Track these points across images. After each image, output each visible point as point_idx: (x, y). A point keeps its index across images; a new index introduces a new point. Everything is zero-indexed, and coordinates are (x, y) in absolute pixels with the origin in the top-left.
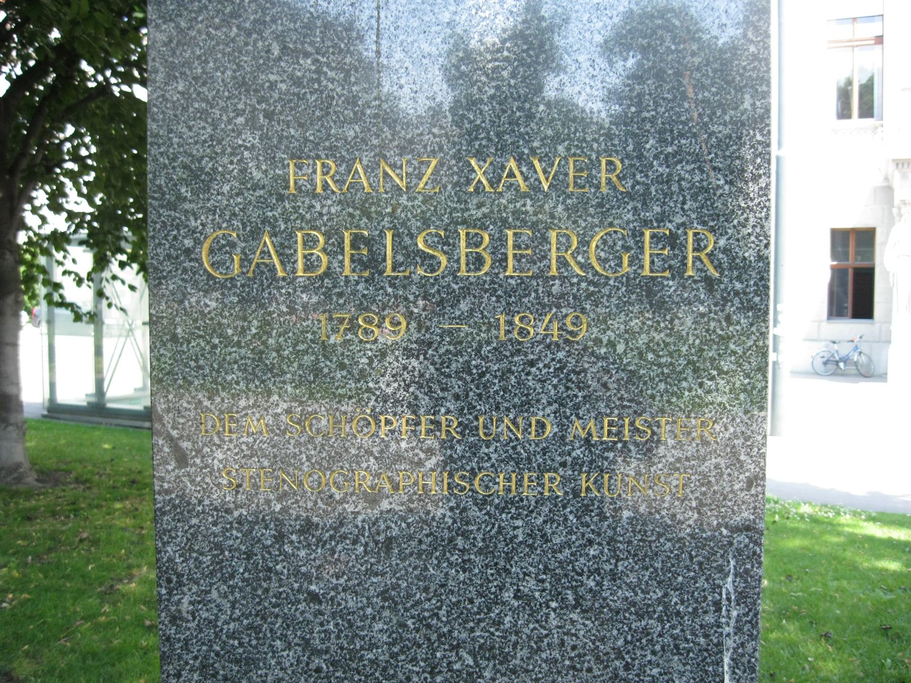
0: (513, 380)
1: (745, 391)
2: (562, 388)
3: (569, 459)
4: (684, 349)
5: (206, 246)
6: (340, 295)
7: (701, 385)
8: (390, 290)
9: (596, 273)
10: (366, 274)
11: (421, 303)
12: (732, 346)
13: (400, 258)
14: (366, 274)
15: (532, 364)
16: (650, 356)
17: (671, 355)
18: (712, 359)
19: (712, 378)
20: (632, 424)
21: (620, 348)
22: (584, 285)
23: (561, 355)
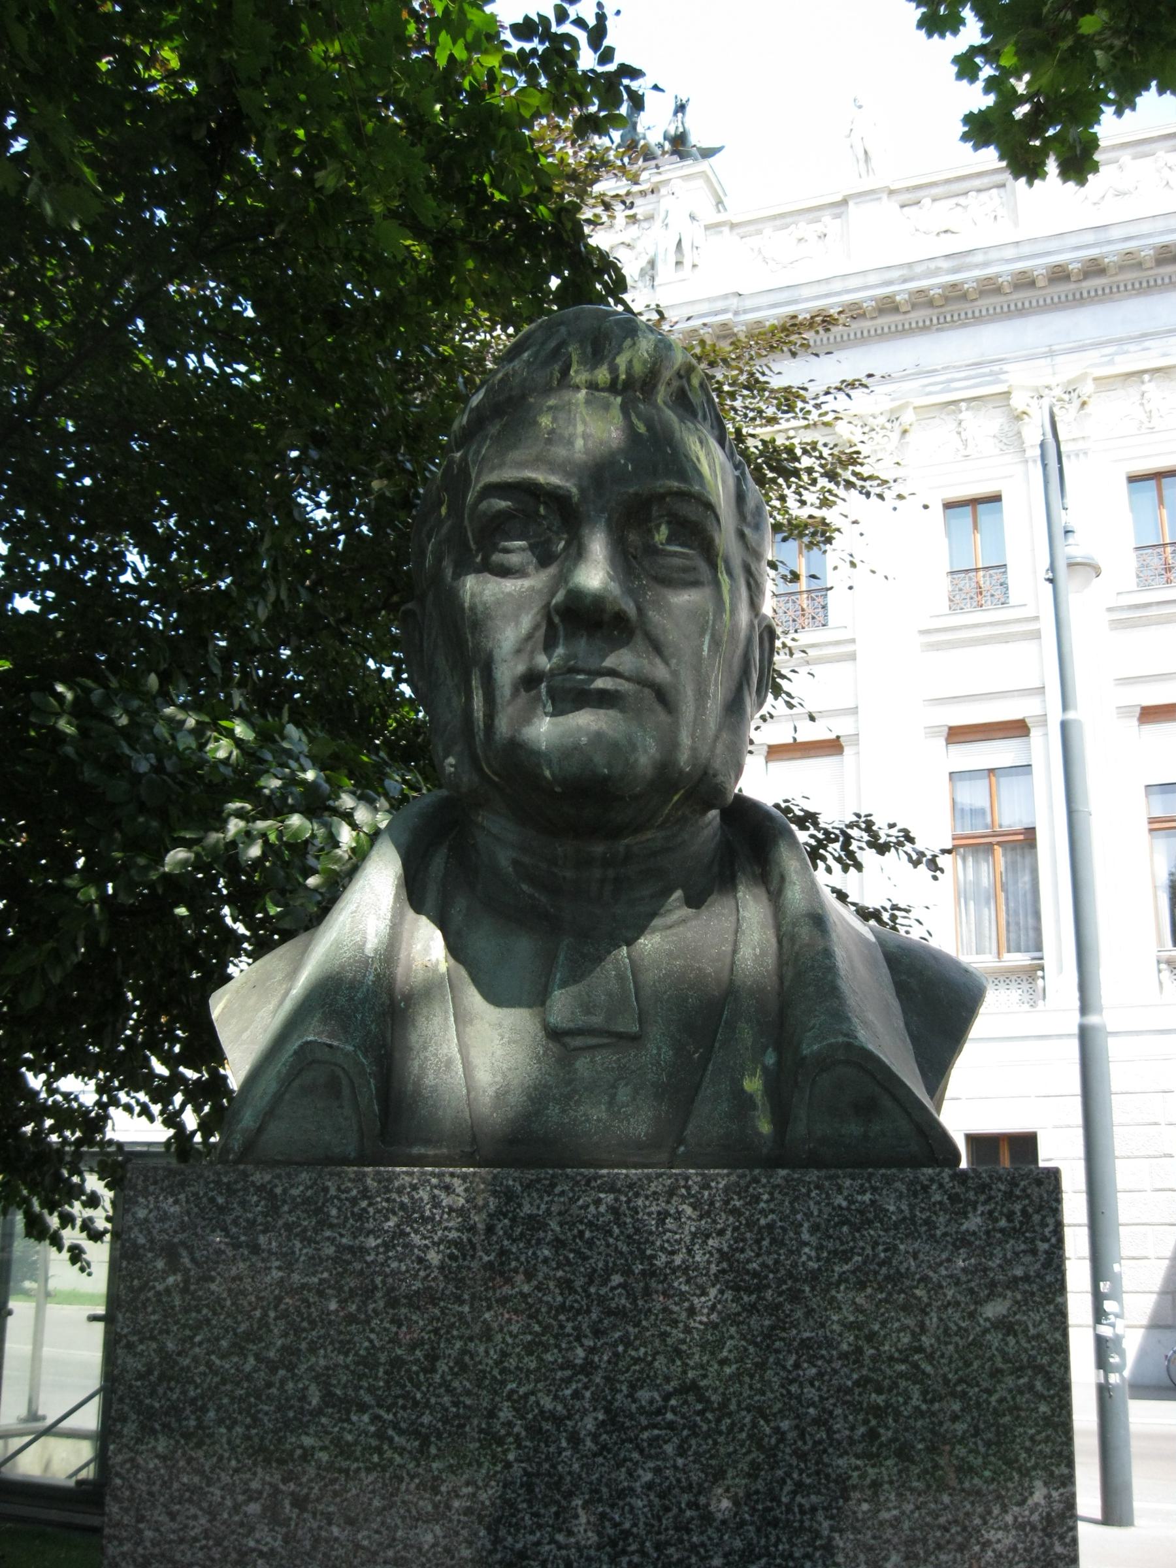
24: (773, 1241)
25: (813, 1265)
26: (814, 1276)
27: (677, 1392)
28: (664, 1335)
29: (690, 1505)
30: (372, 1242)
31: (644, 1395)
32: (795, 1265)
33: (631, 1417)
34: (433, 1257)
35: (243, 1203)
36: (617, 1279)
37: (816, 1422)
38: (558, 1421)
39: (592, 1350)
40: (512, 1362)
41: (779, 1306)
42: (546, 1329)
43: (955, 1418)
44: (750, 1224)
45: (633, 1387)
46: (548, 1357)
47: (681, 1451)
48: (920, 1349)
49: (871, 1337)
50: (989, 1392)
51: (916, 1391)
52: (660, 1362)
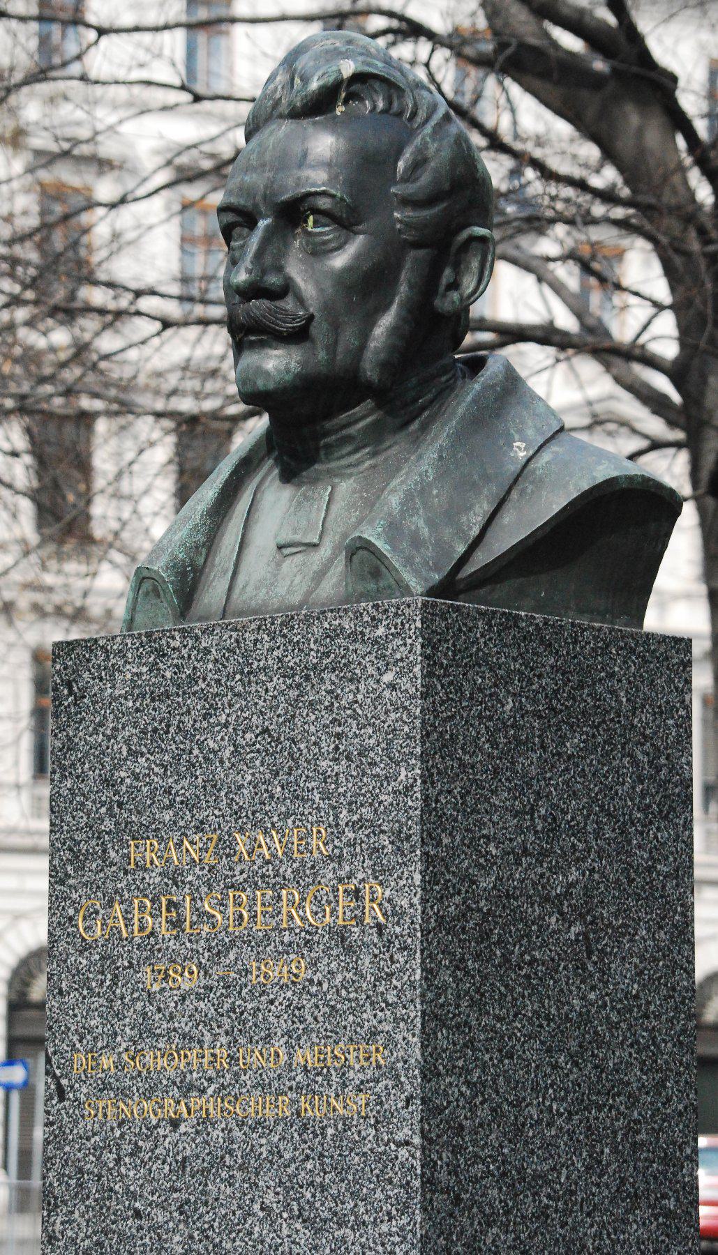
0: (261, 1017)
1: (403, 1020)
2: (290, 1023)
3: (294, 1083)
4: (364, 985)
5: (81, 914)
6: (159, 950)
7: (375, 1016)
8: (188, 945)
9: (310, 925)
10: (175, 933)
11: (206, 954)
12: (394, 982)
13: (195, 918)
14: (175, 933)
15: (272, 1002)
16: (344, 993)
17: (356, 991)
18: (382, 993)
19: (382, 1010)
20: (333, 1052)
21: (325, 986)
22: (303, 934)
23: (289, 994)
25: (315, 661)
27: (261, 733)
28: (256, 704)
29: (266, 791)
30: (145, 669)
31: (248, 736)
34: (168, 674)
36: (238, 677)
37: (315, 744)
38: (215, 752)
39: (228, 715)
40: (198, 725)
41: (300, 684)
42: (211, 706)
43: (370, 737)
45: (244, 732)
46: (212, 721)
48: (356, 702)
50: (384, 722)
51: (354, 724)
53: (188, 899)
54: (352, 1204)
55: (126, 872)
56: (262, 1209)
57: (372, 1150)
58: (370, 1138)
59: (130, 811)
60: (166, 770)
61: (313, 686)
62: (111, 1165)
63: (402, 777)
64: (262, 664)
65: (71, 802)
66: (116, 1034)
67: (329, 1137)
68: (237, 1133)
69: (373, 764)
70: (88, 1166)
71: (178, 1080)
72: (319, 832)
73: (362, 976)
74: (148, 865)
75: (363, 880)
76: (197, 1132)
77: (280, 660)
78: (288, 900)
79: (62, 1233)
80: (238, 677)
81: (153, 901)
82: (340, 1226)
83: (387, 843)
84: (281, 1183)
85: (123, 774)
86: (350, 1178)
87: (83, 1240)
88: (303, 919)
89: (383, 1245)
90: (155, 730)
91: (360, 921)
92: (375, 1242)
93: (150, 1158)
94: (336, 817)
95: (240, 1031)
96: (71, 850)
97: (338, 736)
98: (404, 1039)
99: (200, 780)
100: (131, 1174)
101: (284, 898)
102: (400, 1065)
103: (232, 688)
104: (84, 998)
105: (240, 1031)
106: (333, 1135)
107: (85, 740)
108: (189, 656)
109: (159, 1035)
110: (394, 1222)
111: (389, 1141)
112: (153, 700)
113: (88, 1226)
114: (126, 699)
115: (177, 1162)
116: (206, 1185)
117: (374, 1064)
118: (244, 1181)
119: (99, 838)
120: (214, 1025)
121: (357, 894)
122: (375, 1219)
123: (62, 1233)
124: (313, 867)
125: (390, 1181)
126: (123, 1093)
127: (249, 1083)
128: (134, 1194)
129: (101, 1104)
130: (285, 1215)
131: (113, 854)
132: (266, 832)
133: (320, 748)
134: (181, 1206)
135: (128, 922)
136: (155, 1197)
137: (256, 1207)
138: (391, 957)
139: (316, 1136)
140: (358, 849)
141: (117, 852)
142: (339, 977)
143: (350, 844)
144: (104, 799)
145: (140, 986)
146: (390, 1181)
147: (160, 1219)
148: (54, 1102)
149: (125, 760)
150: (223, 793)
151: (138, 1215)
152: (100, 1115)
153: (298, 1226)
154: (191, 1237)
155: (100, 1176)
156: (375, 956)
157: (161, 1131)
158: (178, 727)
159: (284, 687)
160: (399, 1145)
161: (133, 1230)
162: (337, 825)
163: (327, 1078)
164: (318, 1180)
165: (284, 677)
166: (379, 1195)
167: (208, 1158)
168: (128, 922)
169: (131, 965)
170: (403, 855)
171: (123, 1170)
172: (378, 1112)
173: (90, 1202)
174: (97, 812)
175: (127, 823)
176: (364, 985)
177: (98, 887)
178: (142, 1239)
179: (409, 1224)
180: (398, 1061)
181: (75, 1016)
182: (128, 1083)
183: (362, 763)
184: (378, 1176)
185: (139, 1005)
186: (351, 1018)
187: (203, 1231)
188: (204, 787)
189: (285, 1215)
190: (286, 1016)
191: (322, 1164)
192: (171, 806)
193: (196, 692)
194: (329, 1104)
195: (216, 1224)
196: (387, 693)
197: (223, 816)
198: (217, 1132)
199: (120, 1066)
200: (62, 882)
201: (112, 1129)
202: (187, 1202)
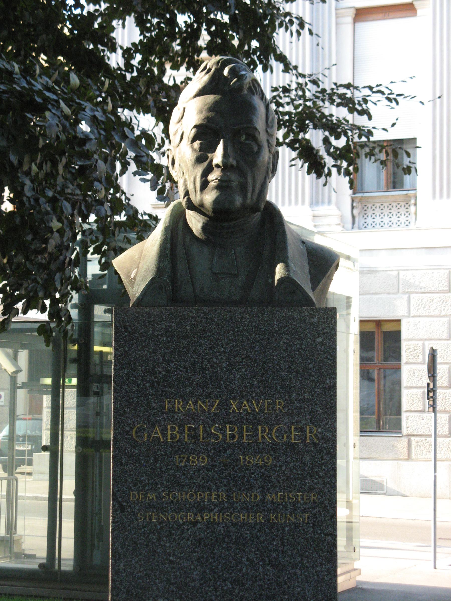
0: (246, 479)
1: (329, 483)
2: (263, 483)
3: (266, 508)
4: (306, 468)
5: (134, 430)
6: (184, 448)
7: (313, 481)
8: (202, 447)
9: (275, 441)
10: (193, 441)
11: (212, 451)
12: (324, 467)
13: (205, 435)
14: (193, 441)
15: (252, 473)
16: (294, 471)
17: (302, 470)
18: (317, 472)
19: (317, 479)
20: (288, 495)
21: (284, 468)
22: (271, 445)
23: (263, 470)
24: (268, 324)
25: (277, 329)
26: (277, 331)
27: (245, 358)
28: (242, 345)
29: (248, 383)
30: (173, 324)
31: (237, 358)
32: (273, 329)
33: (234, 363)
34: (188, 327)
35: (142, 316)
39: (225, 348)
42: (215, 343)
43: (309, 364)
44: (262, 320)
45: (235, 357)
46: (215, 350)
47: (246, 371)
48: (301, 348)
49: (290, 346)
51: (300, 358)
52: (241, 351)
53: (201, 427)
54: (300, 559)
55: (162, 413)
56: (247, 561)
57: (311, 537)
58: (310, 532)
59: (165, 386)
60: (187, 370)
61: (276, 340)
62: (155, 541)
63: (328, 382)
64: (245, 328)
65: (127, 380)
66: (157, 484)
67: (286, 532)
68: (232, 528)
69: (310, 375)
70: (140, 541)
71: (196, 505)
72: (279, 402)
73: (305, 464)
74: (176, 410)
75: (306, 424)
76: (208, 528)
77: (256, 327)
78: (262, 430)
79: (124, 570)
80: (231, 332)
81: (179, 427)
82: (293, 568)
83: (319, 409)
84: (258, 550)
85: (160, 370)
86: (299, 548)
87: (138, 573)
88: (271, 439)
89: (317, 576)
90: (180, 352)
91: (304, 441)
92: (313, 575)
93: (179, 538)
94: (290, 396)
95: (234, 485)
96: (126, 401)
97: (292, 362)
98: (329, 491)
99: (208, 375)
100: (168, 545)
101: (260, 430)
102: (327, 502)
103: (228, 337)
104: (137, 467)
105: (234, 485)
106: (288, 531)
107: (136, 353)
108: (201, 321)
109: (184, 485)
110: (324, 567)
111: (321, 533)
112: (178, 338)
113: (140, 567)
114: (162, 336)
115: (196, 540)
116: (214, 550)
117: (312, 501)
118: (236, 549)
119: (145, 397)
120: (218, 482)
121: (302, 430)
122: (313, 565)
123: (124, 570)
124: (276, 417)
125: (321, 550)
126: (162, 510)
127: (239, 507)
128: (169, 554)
129: (148, 514)
130: (261, 563)
131: (154, 405)
132: (248, 401)
133: (280, 367)
134: (199, 559)
135: (164, 435)
136: (182, 555)
137: (244, 560)
138: (322, 457)
139: (279, 530)
140: (303, 411)
141: (157, 404)
142: (291, 465)
143: (297, 408)
144: (148, 379)
145: (172, 463)
146: (321, 550)
147: (185, 564)
148: (118, 513)
149: (162, 363)
150: (222, 382)
151: (171, 562)
152: (148, 519)
153: (268, 568)
154: (205, 572)
155: (147, 546)
156: (313, 456)
157: (186, 527)
158: (194, 351)
159: (259, 339)
160: (326, 535)
161: (169, 569)
162: (290, 400)
163: (286, 506)
164: (280, 549)
165: (259, 334)
166: (315, 555)
167: (214, 539)
168: (164, 435)
169: (166, 454)
170: (328, 414)
171: (162, 543)
172: (315, 521)
173: (142, 556)
174: (144, 385)
175: (163, 391)
176: (306, 468)
177: (145, 419)
178: (174, 573)
179: (332, 567)
180: (326, 500)
181: (131, 475)
182: (164, 505)
183: (304, 375)
184: (314, 548)
185: (171, 472)
186: (299, 482)
187: (212, 570)
188: (211, 379)
189: (261, 563)
190: (261, 480)
191: (283, 542)
192: (190, 385)
193: (206, 337)
194: (286, 517)
195: (220, 567)
196: (319, 346)
197: (222, 392)
198: (219, 528)
199: (159, 497)
200: (122, 415)
201: (155, 525)
202: (202, 557)
